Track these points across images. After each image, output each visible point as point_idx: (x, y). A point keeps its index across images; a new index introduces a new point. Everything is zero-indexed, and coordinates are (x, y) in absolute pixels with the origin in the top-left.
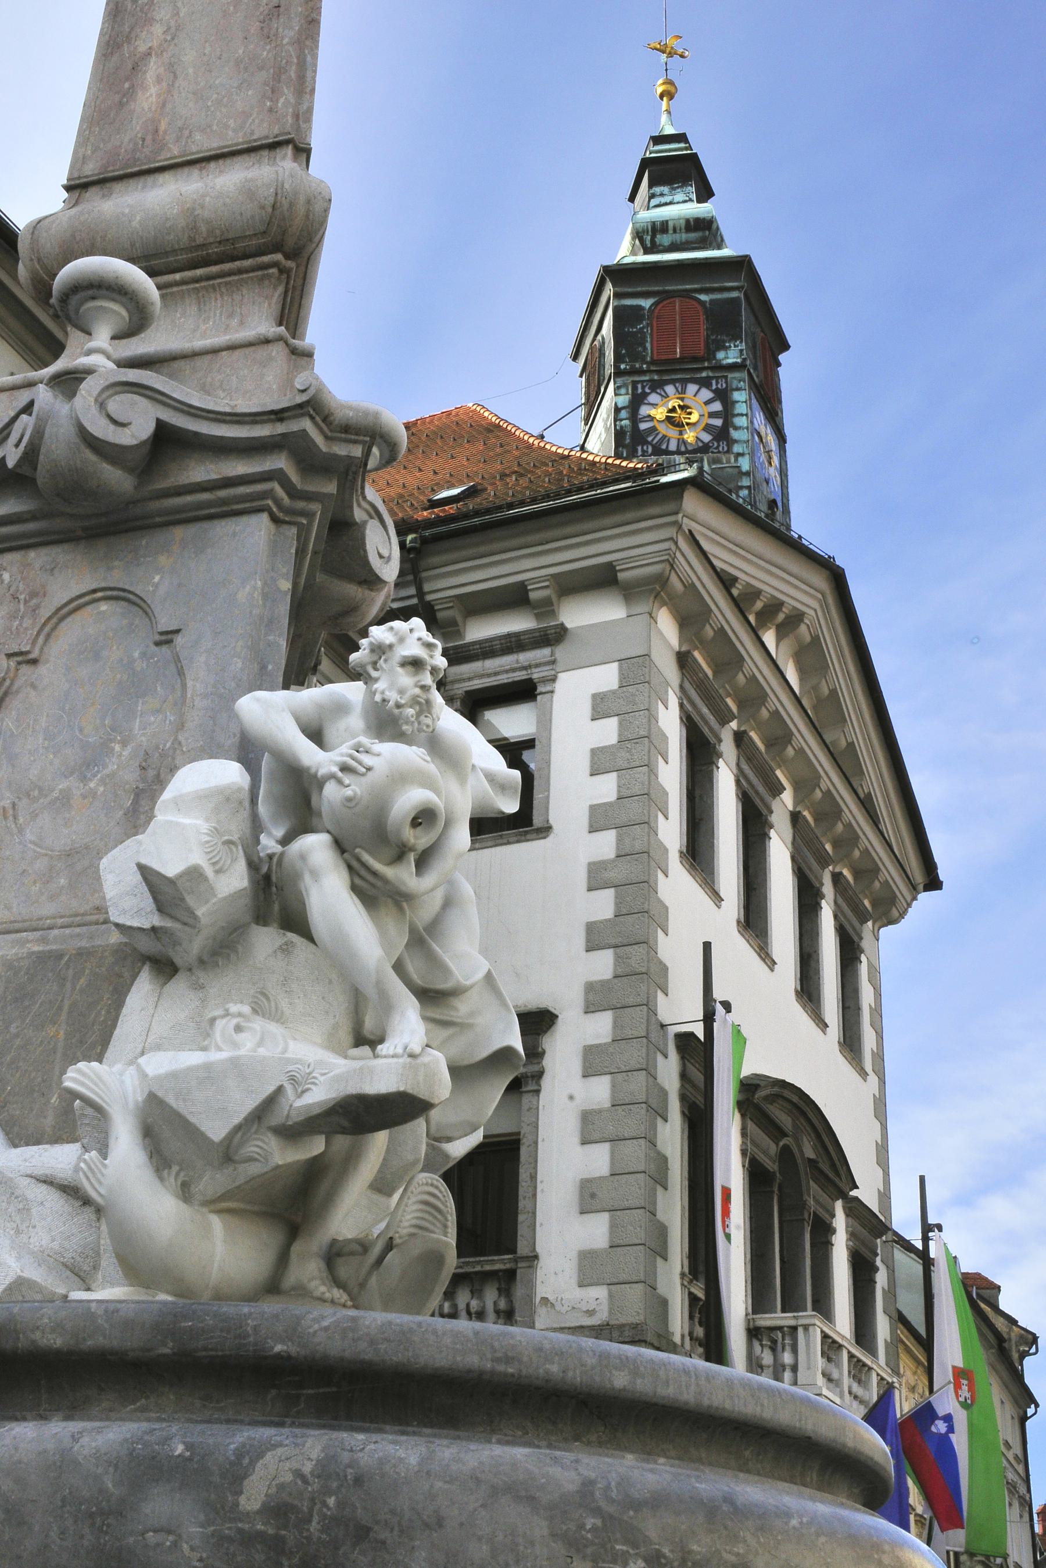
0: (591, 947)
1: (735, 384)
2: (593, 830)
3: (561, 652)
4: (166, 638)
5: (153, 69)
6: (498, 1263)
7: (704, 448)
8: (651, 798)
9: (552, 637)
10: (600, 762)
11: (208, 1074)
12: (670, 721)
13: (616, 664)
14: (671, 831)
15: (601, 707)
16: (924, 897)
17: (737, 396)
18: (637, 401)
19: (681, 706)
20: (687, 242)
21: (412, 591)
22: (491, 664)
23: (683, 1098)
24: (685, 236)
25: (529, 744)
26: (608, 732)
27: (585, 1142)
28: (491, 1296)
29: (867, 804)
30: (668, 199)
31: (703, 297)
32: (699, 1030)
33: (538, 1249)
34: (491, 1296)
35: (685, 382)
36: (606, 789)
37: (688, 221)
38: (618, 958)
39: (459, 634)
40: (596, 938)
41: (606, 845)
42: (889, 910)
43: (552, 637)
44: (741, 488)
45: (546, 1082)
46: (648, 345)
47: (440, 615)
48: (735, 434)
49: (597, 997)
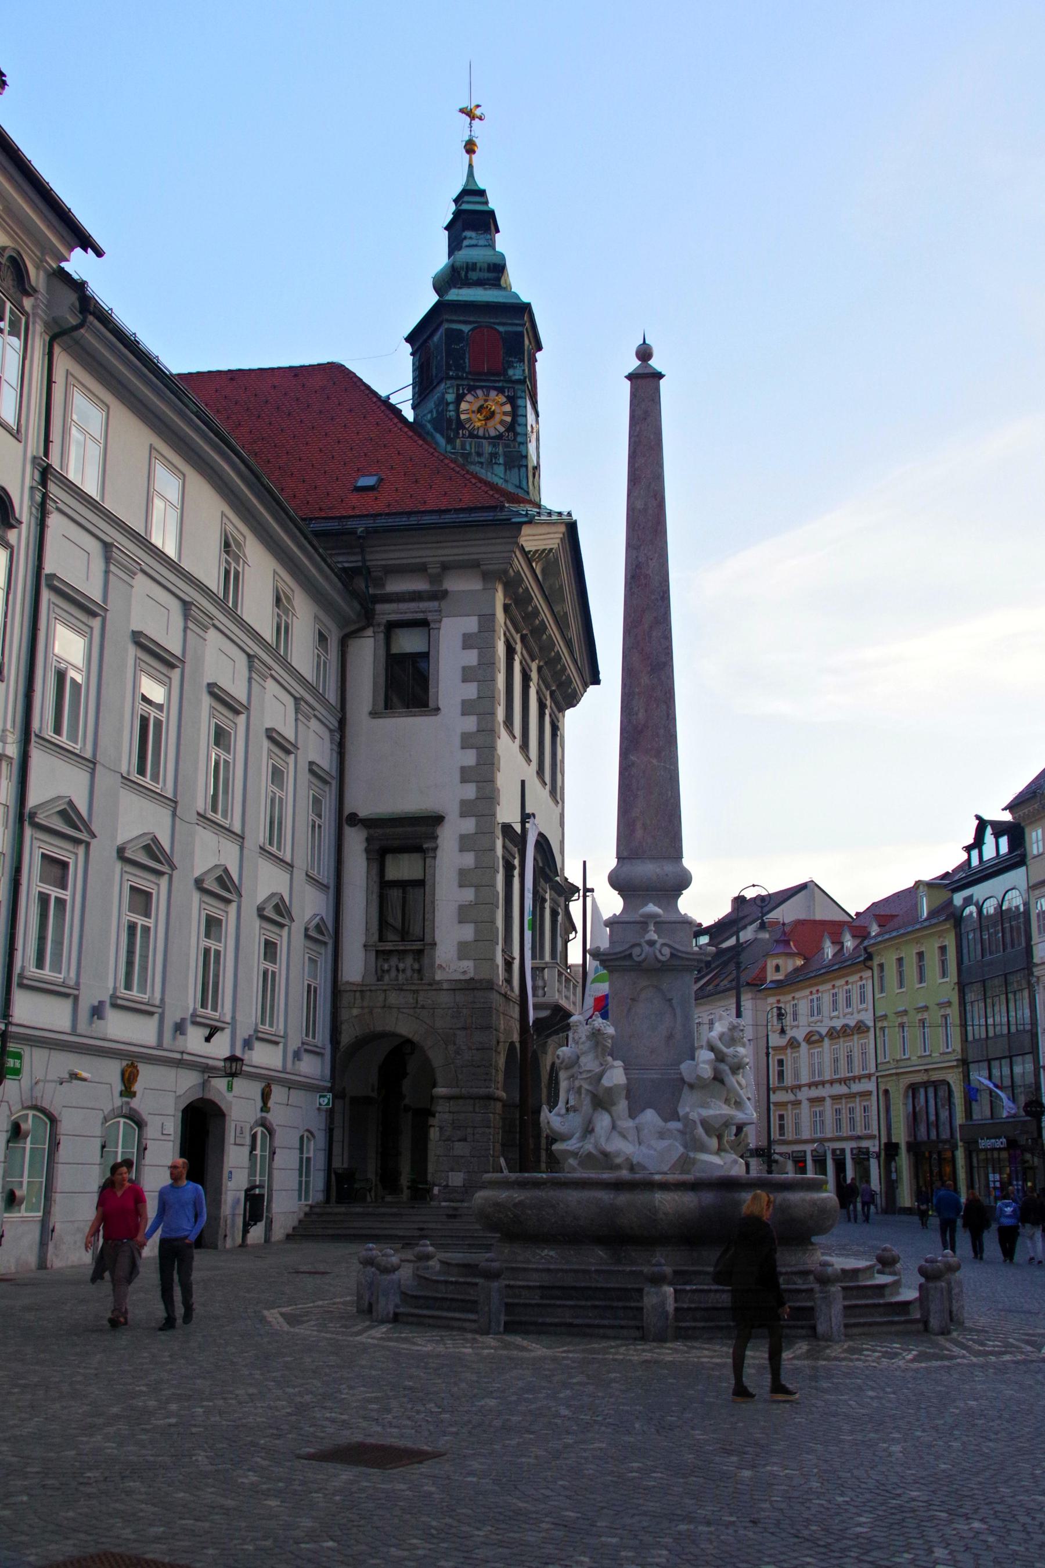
0: (464, 780)
1: (519, 394)
2: (463, 714)
3: (444, 604)
4: (670, 1000)
5: (639, 825)
7: (500, 437)
9: (439, 595)
10: (468, 675)
11: (715, 1116)
13: (476, 618)
15: (468, 642)
16: (592, 688)
17: (520, 402)
19: (505, 634)
20: (488, 279)
21: (359, 558)
22: (403, 606)
23: (504, 858)
24: (487, 275)
27: (461, 886)
28: (409, 960)
29: (569, 644)
30: (473, 242)
31: (501, 329)
32: (518, 828)
33: (437, 939)
34: (409, 960)
35: (489, 388)
36: (471, 691)
37: (489, 265)
38: (478, 788)
39: (383, 586)
41: (470, 724)
42: (572, 700)
43: (439, 595)
44: (522, 466)
45: (439, 853)
46: (467, 361)
47: (374, 574)
48: (519, 429)
49: (467, 809)
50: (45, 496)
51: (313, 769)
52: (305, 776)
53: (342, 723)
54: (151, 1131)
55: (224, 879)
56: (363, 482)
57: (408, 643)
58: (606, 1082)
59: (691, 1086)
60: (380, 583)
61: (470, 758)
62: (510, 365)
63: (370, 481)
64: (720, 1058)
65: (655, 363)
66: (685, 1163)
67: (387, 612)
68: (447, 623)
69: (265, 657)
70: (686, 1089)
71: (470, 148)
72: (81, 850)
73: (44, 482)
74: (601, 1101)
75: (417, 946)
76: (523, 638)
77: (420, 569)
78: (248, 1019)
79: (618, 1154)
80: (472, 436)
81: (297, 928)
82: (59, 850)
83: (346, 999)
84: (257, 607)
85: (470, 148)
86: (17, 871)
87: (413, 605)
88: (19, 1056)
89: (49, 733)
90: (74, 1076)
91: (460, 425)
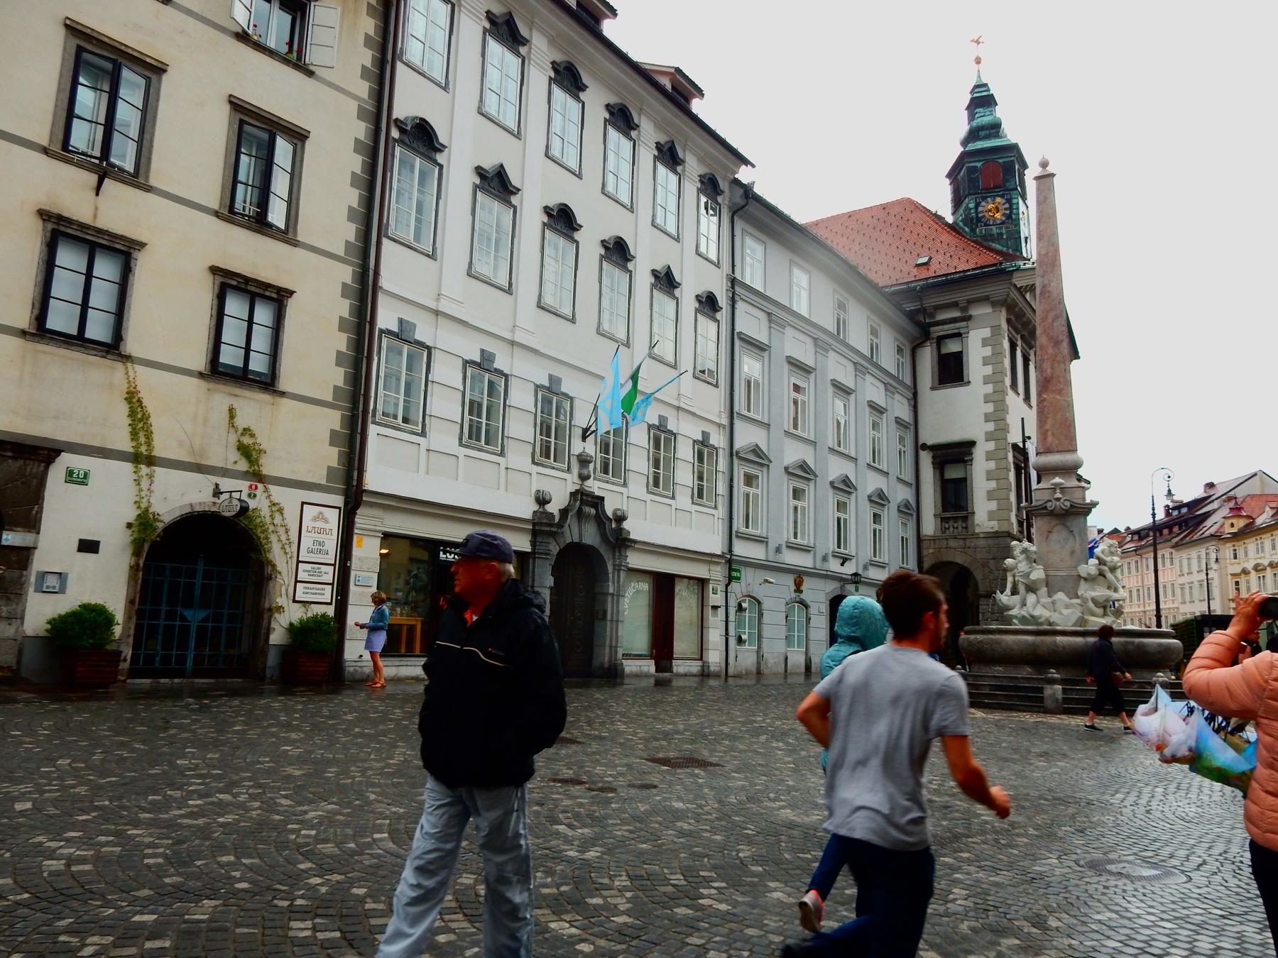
6: (963, 514)
7: (1003, 223)
8: (1002, 373)
9: (968, 318)
10: (986, 361)
12: (1006, 344)
14: (1008, 381)
15: (985, 343)
16: (1075, 362)
17: (1015, 201)
18: (977, 205)
22: (946, 327)
25: (961, 352)
26: (988, 351)
36: (988, 370)
40: (988, 418)
41: (989, 388)
43: (968, 318)
50: (734, 293)
51: (898, 421)
52: (893, 425)
53: (915, 395)
54: (812, 610)
55: (846, 481)
56: (921, 261)
57: (952, 347)
58: (1033, 576)
59: (1085, 579)
60: (932, 315)
61: (990, 408)
62: (1008, 181)
63: (925, 260)
64: (1102, 562)
65: (1050, 169)
66: (1082, 621)
67: (937, 331)
68: (972, 333)
69: (866, 364)
70: (1082, 582)
71: (978, 61)
72: (765, 469)
73: (733, 287)
74: (1031, 589)
75: (963, 514)
76: (1022, 337)
77: (955, 305)
78: (867, 553)
79: (1040, 617)
80: (986, 225)
81: (893, 507)
82: (752, 470)
83: (925, 544)
84: (859, 337)
85: (978, 61)
86: (731, 480)
87: (952, 326)
88: (739, 571)
89: (745, 412)
90: (766, 581)
91: (979, 220)
